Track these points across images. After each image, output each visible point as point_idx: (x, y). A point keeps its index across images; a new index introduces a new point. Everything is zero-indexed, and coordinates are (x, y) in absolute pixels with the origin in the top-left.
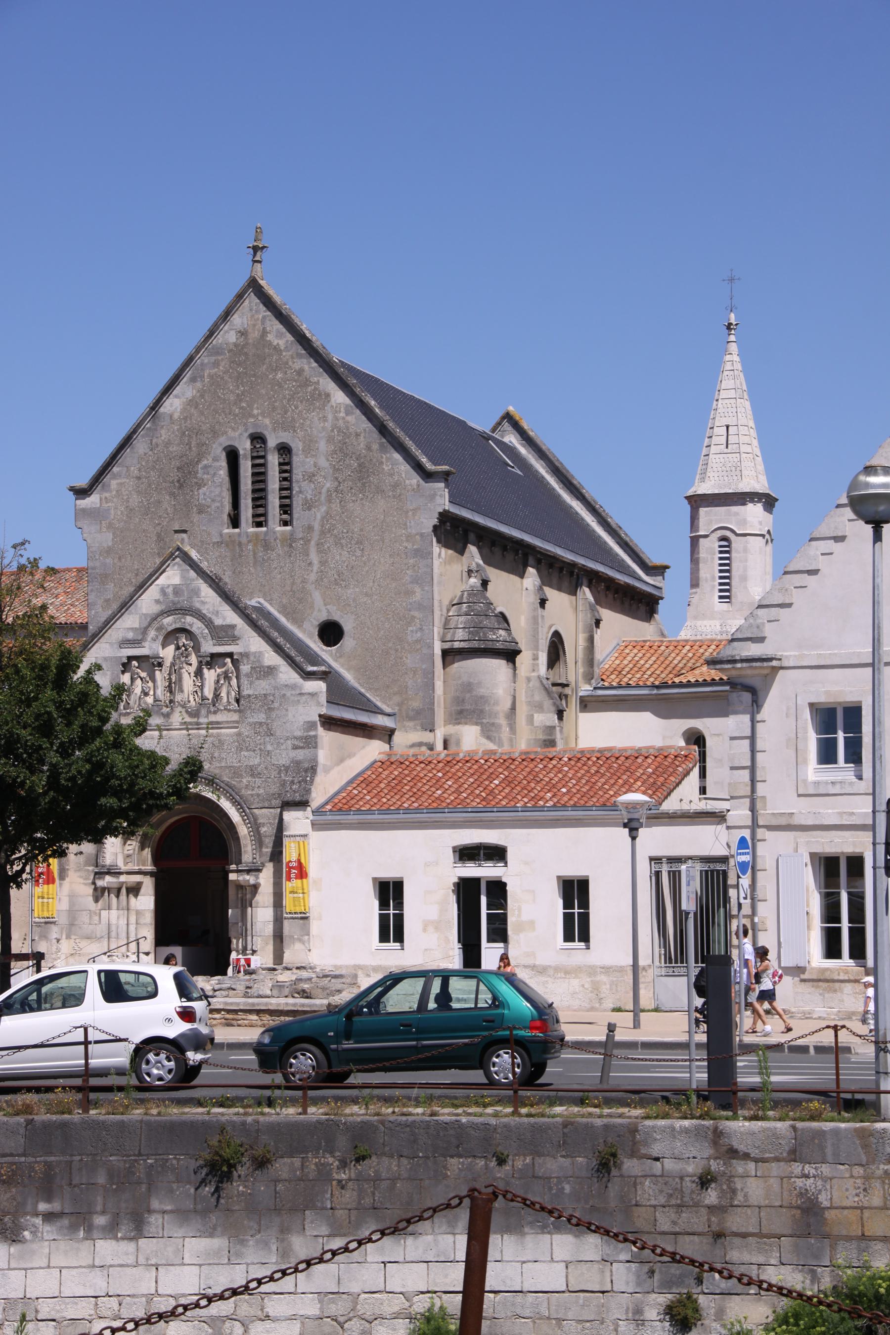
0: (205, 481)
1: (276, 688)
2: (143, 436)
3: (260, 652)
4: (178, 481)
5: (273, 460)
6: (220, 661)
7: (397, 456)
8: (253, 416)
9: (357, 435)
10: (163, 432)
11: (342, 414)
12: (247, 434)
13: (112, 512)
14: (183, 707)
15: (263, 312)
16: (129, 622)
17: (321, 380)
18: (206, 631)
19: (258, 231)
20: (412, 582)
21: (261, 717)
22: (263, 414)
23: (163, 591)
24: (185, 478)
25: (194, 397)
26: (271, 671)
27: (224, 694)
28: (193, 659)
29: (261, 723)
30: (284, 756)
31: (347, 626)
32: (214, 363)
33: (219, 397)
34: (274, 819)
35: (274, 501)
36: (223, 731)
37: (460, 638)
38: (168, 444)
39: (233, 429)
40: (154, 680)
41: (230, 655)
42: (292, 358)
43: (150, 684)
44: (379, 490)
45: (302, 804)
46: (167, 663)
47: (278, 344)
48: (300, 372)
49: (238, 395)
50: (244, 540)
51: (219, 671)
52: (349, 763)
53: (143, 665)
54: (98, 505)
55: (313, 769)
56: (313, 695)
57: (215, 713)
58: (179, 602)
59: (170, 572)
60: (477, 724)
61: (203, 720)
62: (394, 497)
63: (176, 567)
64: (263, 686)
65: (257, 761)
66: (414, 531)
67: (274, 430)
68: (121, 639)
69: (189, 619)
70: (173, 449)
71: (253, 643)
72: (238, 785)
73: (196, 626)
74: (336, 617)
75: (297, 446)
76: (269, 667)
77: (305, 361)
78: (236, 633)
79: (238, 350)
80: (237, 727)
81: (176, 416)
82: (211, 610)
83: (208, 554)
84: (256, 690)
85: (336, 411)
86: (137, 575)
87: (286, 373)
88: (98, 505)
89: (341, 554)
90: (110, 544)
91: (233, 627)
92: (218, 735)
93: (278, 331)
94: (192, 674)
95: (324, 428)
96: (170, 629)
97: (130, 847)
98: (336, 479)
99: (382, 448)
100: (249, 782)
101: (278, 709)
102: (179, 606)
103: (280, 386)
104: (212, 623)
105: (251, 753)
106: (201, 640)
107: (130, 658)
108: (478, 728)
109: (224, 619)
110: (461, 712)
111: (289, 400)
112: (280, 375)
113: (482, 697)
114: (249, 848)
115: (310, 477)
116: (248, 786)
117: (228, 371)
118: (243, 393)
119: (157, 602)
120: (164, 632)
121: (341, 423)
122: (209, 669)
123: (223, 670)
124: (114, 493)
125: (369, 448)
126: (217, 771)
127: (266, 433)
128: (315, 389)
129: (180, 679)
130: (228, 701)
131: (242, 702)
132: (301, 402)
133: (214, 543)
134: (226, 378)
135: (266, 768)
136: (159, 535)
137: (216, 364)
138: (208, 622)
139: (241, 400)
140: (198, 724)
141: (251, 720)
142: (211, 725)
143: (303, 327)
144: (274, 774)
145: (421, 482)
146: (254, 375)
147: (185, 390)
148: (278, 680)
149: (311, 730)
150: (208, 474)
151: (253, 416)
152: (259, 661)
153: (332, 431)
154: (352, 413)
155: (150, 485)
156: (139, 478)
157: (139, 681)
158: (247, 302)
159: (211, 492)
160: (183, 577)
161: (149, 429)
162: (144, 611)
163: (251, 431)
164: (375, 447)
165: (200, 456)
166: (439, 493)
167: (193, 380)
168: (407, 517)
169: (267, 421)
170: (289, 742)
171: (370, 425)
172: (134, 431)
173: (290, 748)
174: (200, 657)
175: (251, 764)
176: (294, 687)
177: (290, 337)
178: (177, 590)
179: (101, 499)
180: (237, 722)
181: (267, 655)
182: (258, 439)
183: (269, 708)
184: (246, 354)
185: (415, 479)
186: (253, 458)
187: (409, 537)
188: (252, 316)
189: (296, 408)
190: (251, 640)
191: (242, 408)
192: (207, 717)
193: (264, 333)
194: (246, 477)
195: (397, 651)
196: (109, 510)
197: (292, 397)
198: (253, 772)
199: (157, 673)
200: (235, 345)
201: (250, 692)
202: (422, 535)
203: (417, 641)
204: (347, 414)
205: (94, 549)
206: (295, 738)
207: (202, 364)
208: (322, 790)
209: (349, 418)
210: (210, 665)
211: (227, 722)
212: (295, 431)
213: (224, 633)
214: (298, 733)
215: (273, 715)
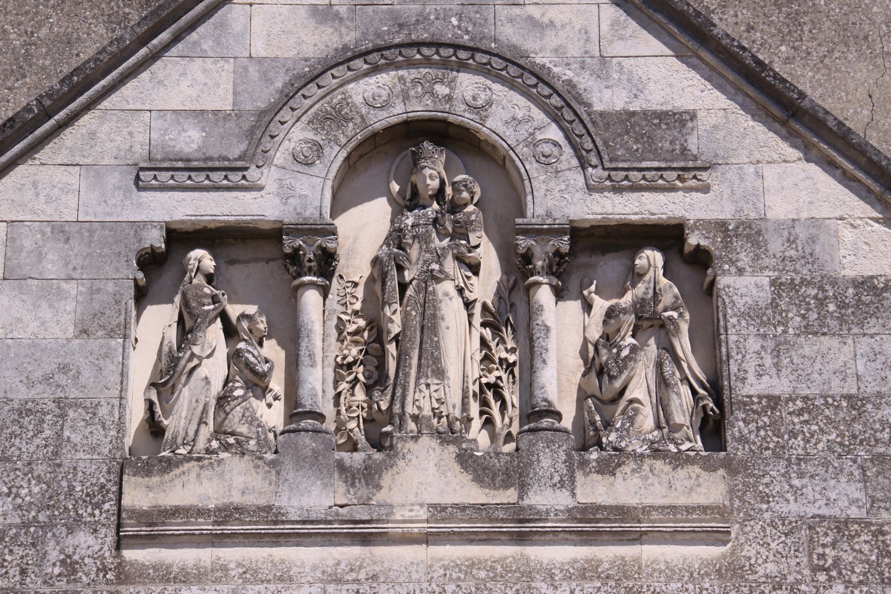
6: (610, 266)
16: (183, 92)
18: (554, 133)
29: (842, 525)
36: (648, 552)
40: (292, 337)
41: (667, 236)
43: (272, 350)
53: (237, 272)
57: (607, 468)
58: (422, 19)
68: (140, 151)
69: (468, 84)
76: (864, 284)
78: (693, 144)
80: (719, 537)
82: (574, 50)
84: (800, 376)
91: (681, 120)
94: (477, 309)
96: (380, 120)
106: (532, 167)
109: (637, 89)
120: (352, 133)
122: (560, 294)
123: (627, 299)
129: (429, 323)
130: (664, 420)
131: (737, 426)
138: (562, 104)
141: (793, 508)
152: (811, 258)
162: (259, 49)
174: (528, 232)
181: (847, 234)
190: (769, 172)
192: (568, 483)
199: (311, 299)
201: (779, 385)
210: (566, 279)
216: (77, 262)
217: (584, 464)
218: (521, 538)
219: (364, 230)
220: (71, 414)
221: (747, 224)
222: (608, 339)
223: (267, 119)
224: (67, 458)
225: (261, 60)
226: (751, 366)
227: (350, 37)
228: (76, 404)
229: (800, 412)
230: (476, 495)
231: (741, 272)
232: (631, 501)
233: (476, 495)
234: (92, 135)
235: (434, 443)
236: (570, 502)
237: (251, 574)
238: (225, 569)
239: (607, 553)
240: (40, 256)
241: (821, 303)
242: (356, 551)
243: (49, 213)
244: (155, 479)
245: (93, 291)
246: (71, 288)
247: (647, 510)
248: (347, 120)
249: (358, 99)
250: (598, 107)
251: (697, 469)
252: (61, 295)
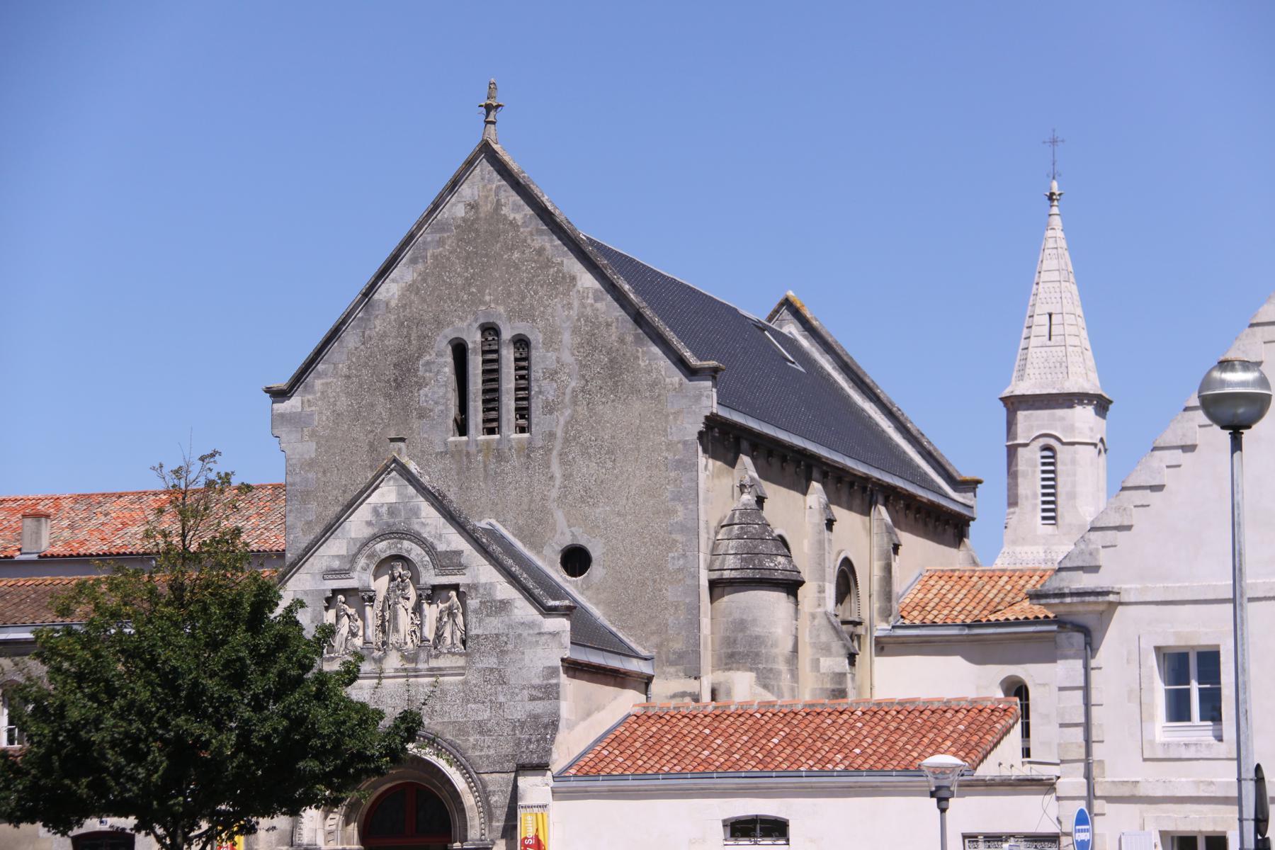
1: (510, 626)
2: (353, 328)
4: (395, 380)
5: (508, 355)
6: (444, 593)
7: (656, 350)
8: (484, 303)
9: (608, 325)
10: (377, 322)
11: (590, 301)
12: (477, 325)
13: (316, 417)
14: (398, 650)
15: (497, 181)
16: (335, 548)
17: (565, 261)
18: (427, 558)
19: (492, 87)
20: (672, 500)
21: (492, 662)
22: (496, 301)
23: (376, 511)
24: (403, 377)
26: (504, 606)
27: (447, 634)
28: (412, 592)
29: (491, 670)
30: (520, 709)
31: (596, 552)
32: (438, 242)
34: (507, 785)
35: (508, 404)
36: (446, 678)
37: (731, 566)
38: (383, 336)
39: (461, 319)
40: (363, 618)
41: (455, 587)
42: (532, 234)
43: (360, 623)
44: (635, 390)
45: (541, 768)
46: (380, 597)
48: (540, 251)
50: (473, 449)
51: (442, 606)
52: (597, 716)
53: (351, 599)
55: (554, 725)
56: (554, 635)
57: (437, 657)
58: (394, 524)
59: (384, 488)
60: (751, 670)
61: (422, 666)
62: (652, 397)
63: (391, 482)
64: (494, 624)
65: (486, 715)
66: (675, 439)
67: (510, 319)
69: (406, 544)
70: (389, 342)
71: (482, 573)
72: (463, 745)
73: (415, 552)
74: (583, 541)
75: (536, 337)
76: (501, 601)
77: (546, 238)
78: (463, 561)
79: (467, 226)
80: (463, 675)
81: (393, 303)
85: (583, 297)
86: (344, 492)
87: (523, 253)
89: (588, 466)
93: (514, 203)
94: (410, 611)
95: (568, 318)
96: (383, 556)
97: (332, 822)
98: (583, 376)
99: (638, 342)
102: (394, 529)
103: (517, 267)
104: (434, 548)
106: (421, 569)
107: (335, 592)
108: (753, 675)
109: (449, 544)
110: (731, 655)
111: (527, 284)
112: (516, 255)
113: (757, 637)
114: (477, 822)
115: (552, 375)
116: (479, 748)
118: (473, 276)
119: (369, 523)
120: (377, 560)
121: (589, 311)
125: (622, 341)
126: (438, 728)
127: (499, 323)
128: (559, 271)
130: (453, 643)
131: (469, 644)
133: (437, 454)
134: (453, 258)
135: (498, 724)
136: (371, 445)
137: (441, 242)
138: (429, 549)
139: (470, 285)
140: (416, 670)
141: (480, 666)
142: (433, 672)
143: (545, 199)
144: (507, 730)
145: (685, 380)
146: (486, 255)
147: (404, 274)
151: (484, 303)
152: (490, 594)
153: (579, 320)
154: (603, 299)
155: (361, 386)
156: (348, 377)
157: (345, 620)
158: (478, 170)
159: (434, 393)
160: (399, 494)
161: (361, 318)
162: (353, 536)
163: (482, 321)
164: (629, 338)
165: (422, 350)
167: (414, 261)
168: (667, 422)
169: (501, 309)
170: (525, 692)
171: (623, 313)
172: (343, 322)
176: (531, 625)
177: (528, 211)
178: (392, 510)
180: (463, 668)
182: (490, 330)
184: (477, 231)
185: (677, 377)
186: (484, 352)
187: (670, 446)
188: (484, 186)
189: (536, 293)
191: (471, 294)
192: (427, 662)
193: (499, 205)
194: (475, 375)
195: (655, 581)
197: (531, 280)
198: (482, 728)
199: (368, 609)
200: (464, 220)
201: (479, 632)
202: (685, 443)
203: (680, 570)
204: (596, 301)
205: (294, 461)
206: (533, 687)
207: (424, 243)
208: (566, 749)
209: (598, 305)
210: (431, 599)
212: (534, 320)
213: (449, 561)
214: (537, 682)
215: (507, 659)
218: (416, 676)
219: (381, 586)
222: (441, 619)
227: (376, 530)
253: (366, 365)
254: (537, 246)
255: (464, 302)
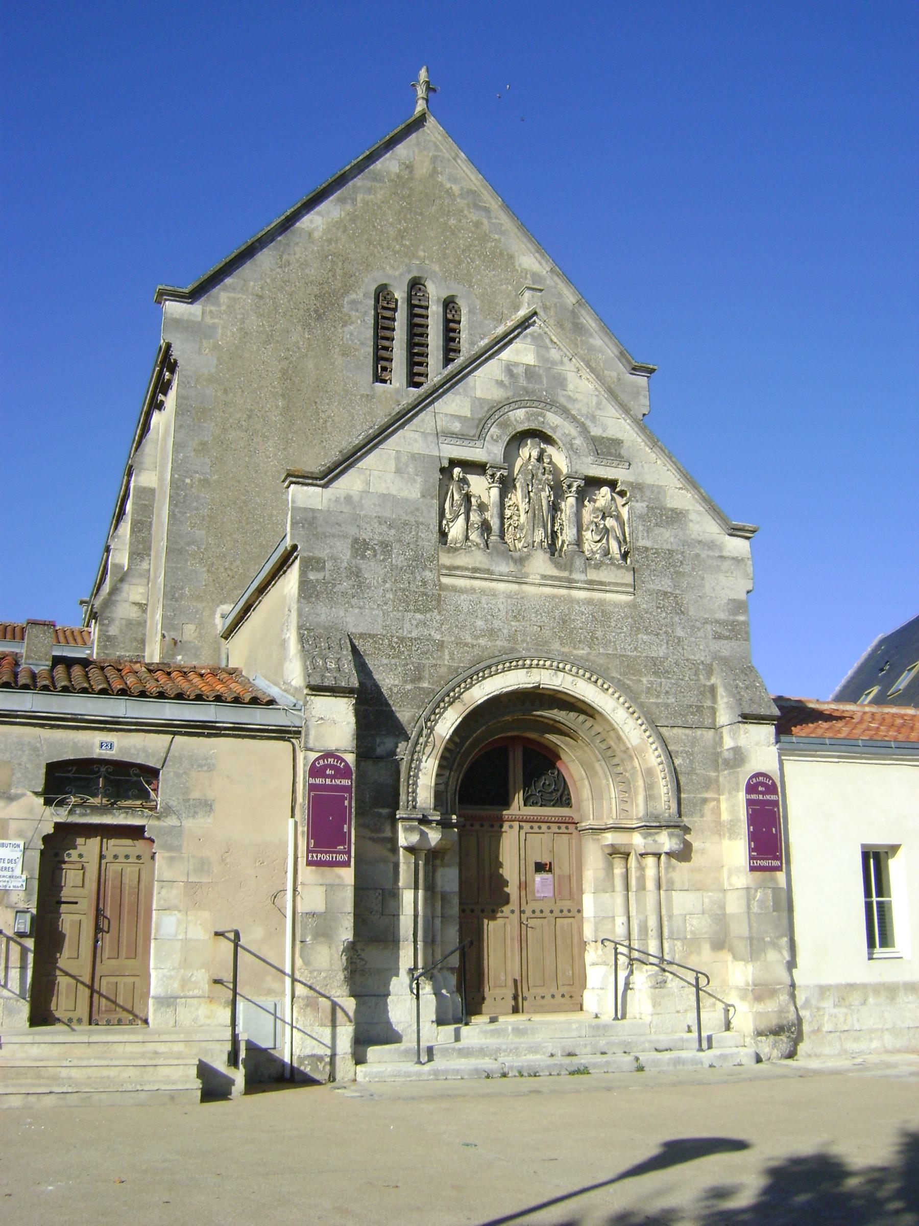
0: (354, 319)
1: (685, 543)
3: (660, 487)
8: (418, 258)
10: (297, 249)
21: (665, 584)
23: (509, 369)
25: (341, 220)
26: (676, 517)
29: (665, 593)
33: (374, 226)
36: (609, 596)
38: (304, 265)
39: (392, 267)
41: (612, 484)
47: (451, 188)
49: (400, 231)
54: (199, 319)
56: (738, 561)
64: (666, 537)
65: (662, 651)
70: (311, 272)
72: (635, 687)
76: (673, 510)
78: (623, 452)
79: (400, 183)
83: (354, 408)
87: (460, 221)
88: (199, 319)
90: (213, 370)
91: (618, 442)
92: (602, 602)
100: (652, 683)
101: (690, 575)
105: (654, 638)
107: (454, 463)
112: (452, 222)
117: (388, 202)
119: (500, 383)
120: (511, 431)
124: (224, 308)
128: (496, 247)
132: (479, 256)
133: (362, 396)
136: (284, 372)
139: (402, 237)
140: (570, 581)
141: (652, 586)
146: (421, 214)
148: (687, 532)
149: (738, 613)
150: (357, 310)
151: (418, 258)
152: (658, 499)
160: (539, 356)
162: (479, 394)
165: (347, 289)
166: (643, 393)
167: (342, 201)
170: (708, 627)
173: (710, 637)
175: (654, 654)
176: (711, 545)
178: (530, 372)
179: (203, 313)
183: (676, 572)
189: (473, 261)
191: (404, 246)
192: (584, 571)
196: (214, 327)
198: (656, 667)
200: (398, 176)
201: (648, 544)
206: (717, 622)
211: (616, 584)
214: (722, 616)
216: (419, 469)
217: (590, 565)
220: (421, 527)
221: (640, 484)
223: (483, 422)
224: (420, 543)
225: (479, 399)
226: (640, 535)
227: (510, 394)
228: (422, 524)
229: (654, 554)
230: (555, 572)
231: (637, 501)
232: (604, 580)
233: (555, 572)
234: (423, 420)
235: (542, 552)
236: (586, 579)
237: (483, 592)
238: (474, 590)
239: (597, 595)
240: (407, 466)
241: (661, 515)
242: (515, 587)
243: (409, 449)
244: (451, 555)
245: (426, 481)
246: (419, 479)
247: (609, 584)
248: (510, 425)
249: (512, 419)
250: (592, 434)
251: (624, 571)
252: (415, 481)
253: (281, 289)
254: (475, 219)
255: (395, 253)
